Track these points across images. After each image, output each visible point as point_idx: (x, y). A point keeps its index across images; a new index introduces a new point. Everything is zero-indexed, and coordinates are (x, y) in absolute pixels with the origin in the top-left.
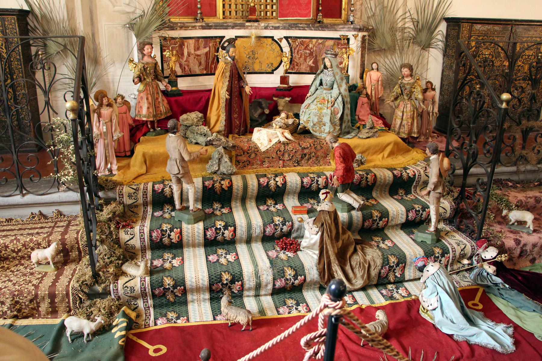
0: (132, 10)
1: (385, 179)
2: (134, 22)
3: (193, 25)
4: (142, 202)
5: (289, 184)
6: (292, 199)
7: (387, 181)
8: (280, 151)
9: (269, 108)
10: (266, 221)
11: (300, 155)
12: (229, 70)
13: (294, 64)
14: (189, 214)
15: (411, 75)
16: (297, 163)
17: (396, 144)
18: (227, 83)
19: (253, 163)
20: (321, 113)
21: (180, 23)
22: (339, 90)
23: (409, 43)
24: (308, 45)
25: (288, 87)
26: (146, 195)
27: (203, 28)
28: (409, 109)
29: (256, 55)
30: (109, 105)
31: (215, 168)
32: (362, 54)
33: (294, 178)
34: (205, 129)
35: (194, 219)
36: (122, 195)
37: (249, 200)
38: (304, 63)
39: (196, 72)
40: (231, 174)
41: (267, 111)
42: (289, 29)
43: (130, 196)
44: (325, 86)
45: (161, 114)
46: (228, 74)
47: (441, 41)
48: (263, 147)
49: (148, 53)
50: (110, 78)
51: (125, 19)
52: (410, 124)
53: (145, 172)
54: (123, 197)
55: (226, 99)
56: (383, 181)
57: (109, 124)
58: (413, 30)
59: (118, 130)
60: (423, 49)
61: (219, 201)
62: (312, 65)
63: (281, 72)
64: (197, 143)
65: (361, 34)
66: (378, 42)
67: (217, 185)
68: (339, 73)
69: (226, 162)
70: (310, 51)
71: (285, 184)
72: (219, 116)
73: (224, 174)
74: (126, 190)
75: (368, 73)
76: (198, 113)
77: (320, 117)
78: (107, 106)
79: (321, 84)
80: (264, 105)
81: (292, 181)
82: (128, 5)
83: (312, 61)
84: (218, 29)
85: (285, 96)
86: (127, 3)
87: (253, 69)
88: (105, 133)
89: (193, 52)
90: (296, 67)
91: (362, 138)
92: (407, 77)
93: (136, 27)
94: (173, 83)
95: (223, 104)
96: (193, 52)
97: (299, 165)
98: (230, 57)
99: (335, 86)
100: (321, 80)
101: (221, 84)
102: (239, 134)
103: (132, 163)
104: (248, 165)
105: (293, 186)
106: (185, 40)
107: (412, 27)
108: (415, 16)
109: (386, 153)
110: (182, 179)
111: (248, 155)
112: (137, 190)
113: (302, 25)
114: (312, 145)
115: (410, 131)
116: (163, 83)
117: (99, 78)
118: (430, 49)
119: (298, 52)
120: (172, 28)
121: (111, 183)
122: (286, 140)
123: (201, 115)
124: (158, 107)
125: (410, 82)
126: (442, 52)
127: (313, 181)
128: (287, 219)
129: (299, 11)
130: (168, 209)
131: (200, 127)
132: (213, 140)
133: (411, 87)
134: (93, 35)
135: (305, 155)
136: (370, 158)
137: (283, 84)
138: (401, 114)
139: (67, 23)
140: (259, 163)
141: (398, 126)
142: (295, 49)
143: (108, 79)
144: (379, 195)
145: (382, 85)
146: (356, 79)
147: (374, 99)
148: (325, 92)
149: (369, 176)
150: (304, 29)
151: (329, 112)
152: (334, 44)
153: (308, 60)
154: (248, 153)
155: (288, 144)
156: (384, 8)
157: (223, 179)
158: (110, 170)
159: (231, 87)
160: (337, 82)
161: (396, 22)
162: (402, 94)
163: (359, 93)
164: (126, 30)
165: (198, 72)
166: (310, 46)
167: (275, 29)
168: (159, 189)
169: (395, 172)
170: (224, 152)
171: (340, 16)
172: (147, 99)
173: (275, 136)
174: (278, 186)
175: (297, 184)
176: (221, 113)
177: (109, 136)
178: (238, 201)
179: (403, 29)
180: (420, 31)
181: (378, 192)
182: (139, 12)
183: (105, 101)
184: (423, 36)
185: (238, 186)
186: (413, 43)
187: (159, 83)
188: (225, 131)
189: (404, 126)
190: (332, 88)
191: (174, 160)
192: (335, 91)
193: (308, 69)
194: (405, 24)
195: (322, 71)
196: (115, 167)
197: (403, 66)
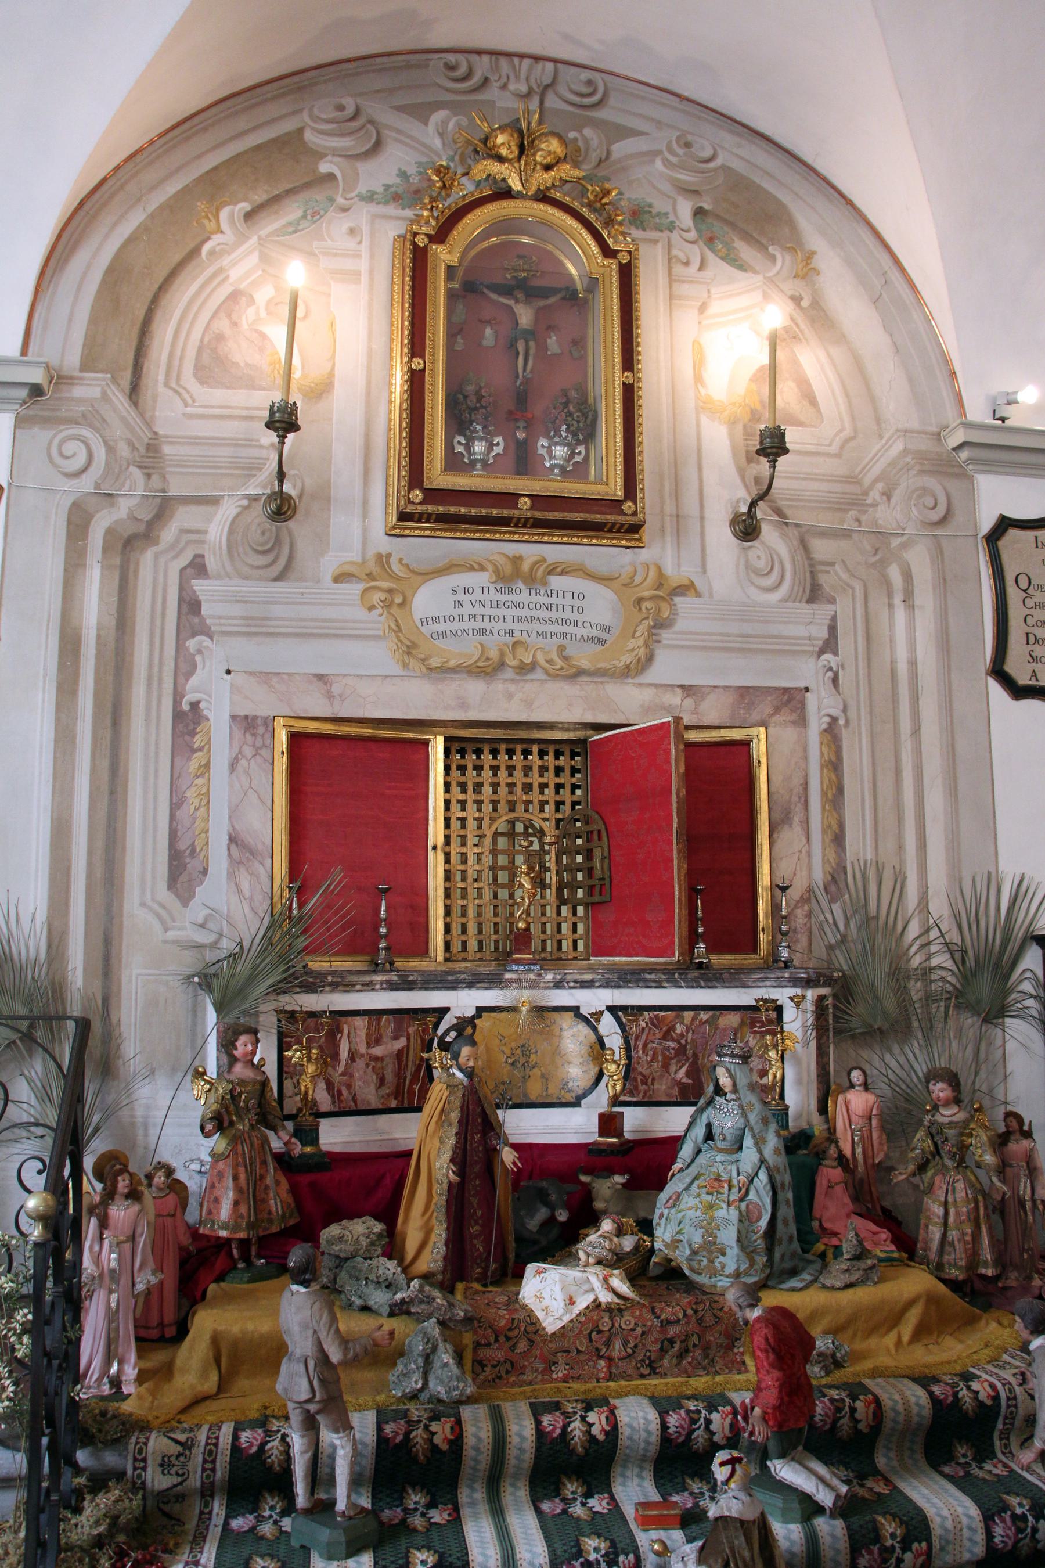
0: (210, 938)
1: (908, 1410)
2: (212, 970)
3: (367, 978)
4: (198, 1484)
5: (625, 1432)
6: (636, 1481)
7: (916, 1419)
8: (599, 1332)
9: (568, 1206)
10: (559, 1552)
11: (655, 1342)
12: (458, 1103)
13: (635, 1079)
14: (332, 1525)
15: (957, 1101)
16: (650, 1365)
17: (932, 1299)
18: (452, 1141)
19: (524, 1367)
20: (712, 1218)
21: (333, 973)
22: (760, 1152)
23: (947, 1008)
24: (672, 1028)
25: (622, 1144)
26: (214, 1462)
27: (393, 987)
28: (961, 1194)
29: (533, 1056)
30: (134, 1195)
31: (415, 1382)
32: (819, 1047)
33: (641, 1414)
34: (390, 1268)
35: (349, 1543)
36: (144, 1460)
37: (508, 1481)
38: (661, 1076)
39: (369, 1103)
40: (460, 1402)
41: (562, 1216)
42: (619, 987)
43: (165, 1464)
44: (720, 1144)
45: (270, 1221)
46: (455, 1116)
47: (1032, 996)
48: (550, 1319)
49: (245, 1055)
50: (139, 1112)
51: (189, 961)
52: (968, 1238)
53: (214, 1390)
54: (144, 1469)
55: (451, 1185)
56: (901, 1418)
57: (128, 1246)
58: (953, 974)
59: (151, 1264)
60: (986, 1020)
61: (421, 1483)
62: (684, 1080)
63: (600, 1100)
64: (365, 1309)
65: (811, 994)
66: (860, 1012)
67: (418, 1435)
68: (758, 1106)
69: (446, 1365)
70: (679, 1043)
71: (613, 1431)
72: (428, 1232)
73: (440, 1401)
74: (157, 1444)
75: (840, 1098)
76: (371, 1221)
77: (710, 1229)
78: (127, 1196)
79: (709, 1136)
80: (554, 1197)
81: (635, 1424)
82: (202, 926)
83: (684, 1070)
84: (433, 989)
85: (609, 1171)
86: (200, 921)
87: (525, 1095)
88: (113, 1271)
89: (363, 1049)
90: (642, 1088)
91: (833, 1288)
92: (947, 1104)
93: (217, 985)
94: (308, 1134)
95: (440, 1198)
96: (363, 1049)
97: (654, 1372)
98: (461, 1070)
99: (748, 1142)
100: (709, 1126)
101: (436, 1143)
102: (483, 1280)
103: (179, 1362)
104: (507, 1372)
105: (636, 1437)
106: (343, 1019)
107: (949, 964)
108: (954, 937)
109: (907, 1330)
110: (319, 1417)
111: (508, 1344)
112: (187, 1446)
113: (653, 976)
114: (690, 1312)
115: (973, 1260)
116: (282, 1133)
117: (109, 1113)
118: (1007, 1020)
119: (645, 1045)
120: (310, 988)
121: (115, 1422)
122: (616, 1300)
123: (378, 1227)
124: (265, 1201)
125: (955, 1119)
126: (1040, 1026)
127: (694, 1421)
128: (620, 1546)
129: (644, 941)
130: (272, 1508)
131: (374, 1262)
132: (412, 1301)
133: (962, 1134)
134: (106, 1000)
135: (672, 1342)
136: (859, 1345)
137: (608, 1136)
138: (940, 1211)
139: (44, 969)
140: (540, 1366)
141: (935, 1245)
142: (636, 1039)
143: (133, 1116)
144: (895, 1463)
145: (882, 1128)
146: (809, 1114)
147: (861, 1168)
148: (720, 1158)
149: (859, 1404)
150: (660, 986)
151: (734, 1214)
152: (742, 1024)
153: (673, 1068)
154: (508, 1339)
155: (620, 1310)
156: (868, 921)
157: (435, 1417)
158: (116, 1383)
159: (465, 1150)
160: (751, 1129)
161: (903, 955)
162: (937, 1152)
163: (817, 1154)
164: (191, 988)
165: (375, 1103)
166: (678, 1031)
167: (582, 987)
168: (252, 1445)
169: (936, 1389)
170: (442, 1334)
171: (754, 948)
172: (235, 1178)
173: (586, 1287)
174: (593, 1439)
175: (649, 1433)
176: (434, 1221)
177: (125, 1280)
178: (478, 1486)
179: (926, 972)
180: (974, 974)
181: (892, 1454)
182: (227, 945)
183: (123, 1184)
184: (984, 986)
185: (479, 1439)
186: (957, 1007)
187: (271, 1134)
188: (444, 1272)
189: (952, 1244)
190: (740, 1148)
191: (298, 1360)
192: (749, 1156)
193: (675, 1091)
194: (928, 959)
195: (710, 1102)
196: (131, 1372)
197: (933, 1076)
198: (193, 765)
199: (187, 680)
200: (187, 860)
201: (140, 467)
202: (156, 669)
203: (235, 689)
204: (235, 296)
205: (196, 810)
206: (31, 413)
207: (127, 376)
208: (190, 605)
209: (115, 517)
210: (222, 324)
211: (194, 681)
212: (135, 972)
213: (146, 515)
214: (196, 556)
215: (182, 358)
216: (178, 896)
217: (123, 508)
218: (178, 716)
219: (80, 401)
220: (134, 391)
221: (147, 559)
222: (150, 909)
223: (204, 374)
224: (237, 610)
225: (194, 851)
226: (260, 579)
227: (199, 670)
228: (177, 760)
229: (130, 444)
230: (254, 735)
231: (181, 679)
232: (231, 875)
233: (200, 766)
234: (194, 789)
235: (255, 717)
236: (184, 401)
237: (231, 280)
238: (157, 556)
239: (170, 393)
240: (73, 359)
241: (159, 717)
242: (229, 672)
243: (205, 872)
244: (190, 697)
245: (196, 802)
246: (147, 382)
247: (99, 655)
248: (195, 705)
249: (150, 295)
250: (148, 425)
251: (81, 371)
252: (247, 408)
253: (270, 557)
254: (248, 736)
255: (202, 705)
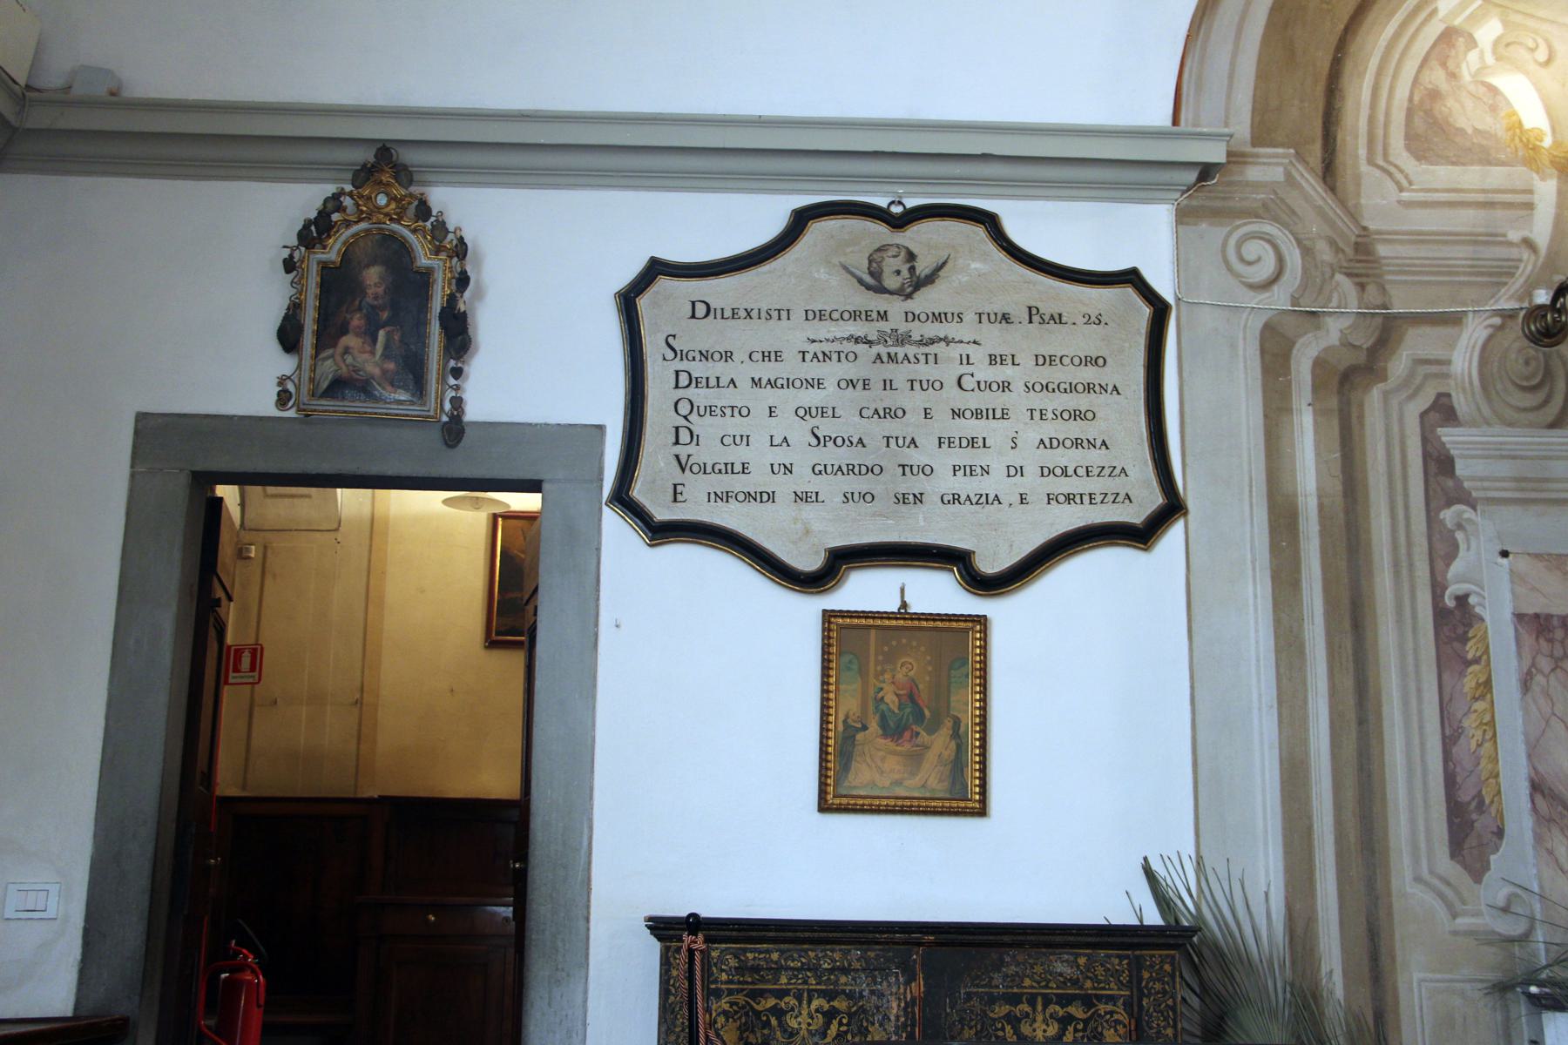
0: (1515, 928)
82: (1505, 910)
86: (1501, 902)
134: (1379, 1016)
198: (1469, 683)
199: (1448, 565)
200: (1474, 816)
201: (1349, 275)
202: (1403, 550)
203: (1513, 574)
204: (1448, 36)
205: (1479, 745)
206: (1194, 203)
207: (1316, 151)
208: (1439, 463)
209: (1323, 344)
210: (1436, 77)
211: (1457, 567)
212: (1416, 976)
213: (1365, 340)
214: (1440, 395)
215: (1386, 125)
216: (1466, 867)
217: (1334, 331)
218: (1440, 614)
219: (1256, 186)
220: (1329, 171)
221: (1374, 398)
222: (1427, 884)
223: (1419, 146)
224: (1504, 469)
225: (1481, 802)
226: (1531, 425)
227: (1462, 553)
228: (1446, 676)
229: (1332, 243)
230: (1551, 641)
231: (1440, 564)
232: (1539, 839)
233: (1478, 685)
234: (1473, 716)
235: (1549, 617)
236: (1397, 183)
237: (1441, 14)
238: (1386, 395)
239: (1378, 173)
240: (1242, 127)
241: (1414, 617)
242: (1505, 554)
243: (1500, 833)
244: (1454, 589)
245: (1479, 734)
246: (1343, 158)
247: (1323, 533)
248: (1462, 600)
249: (1333, 40)
250: (1354, 215)
251: (1254, 145)
252: (1484, 191)
253: (1540, 396)
254: (1542, 642)
255: (1472, 600)
